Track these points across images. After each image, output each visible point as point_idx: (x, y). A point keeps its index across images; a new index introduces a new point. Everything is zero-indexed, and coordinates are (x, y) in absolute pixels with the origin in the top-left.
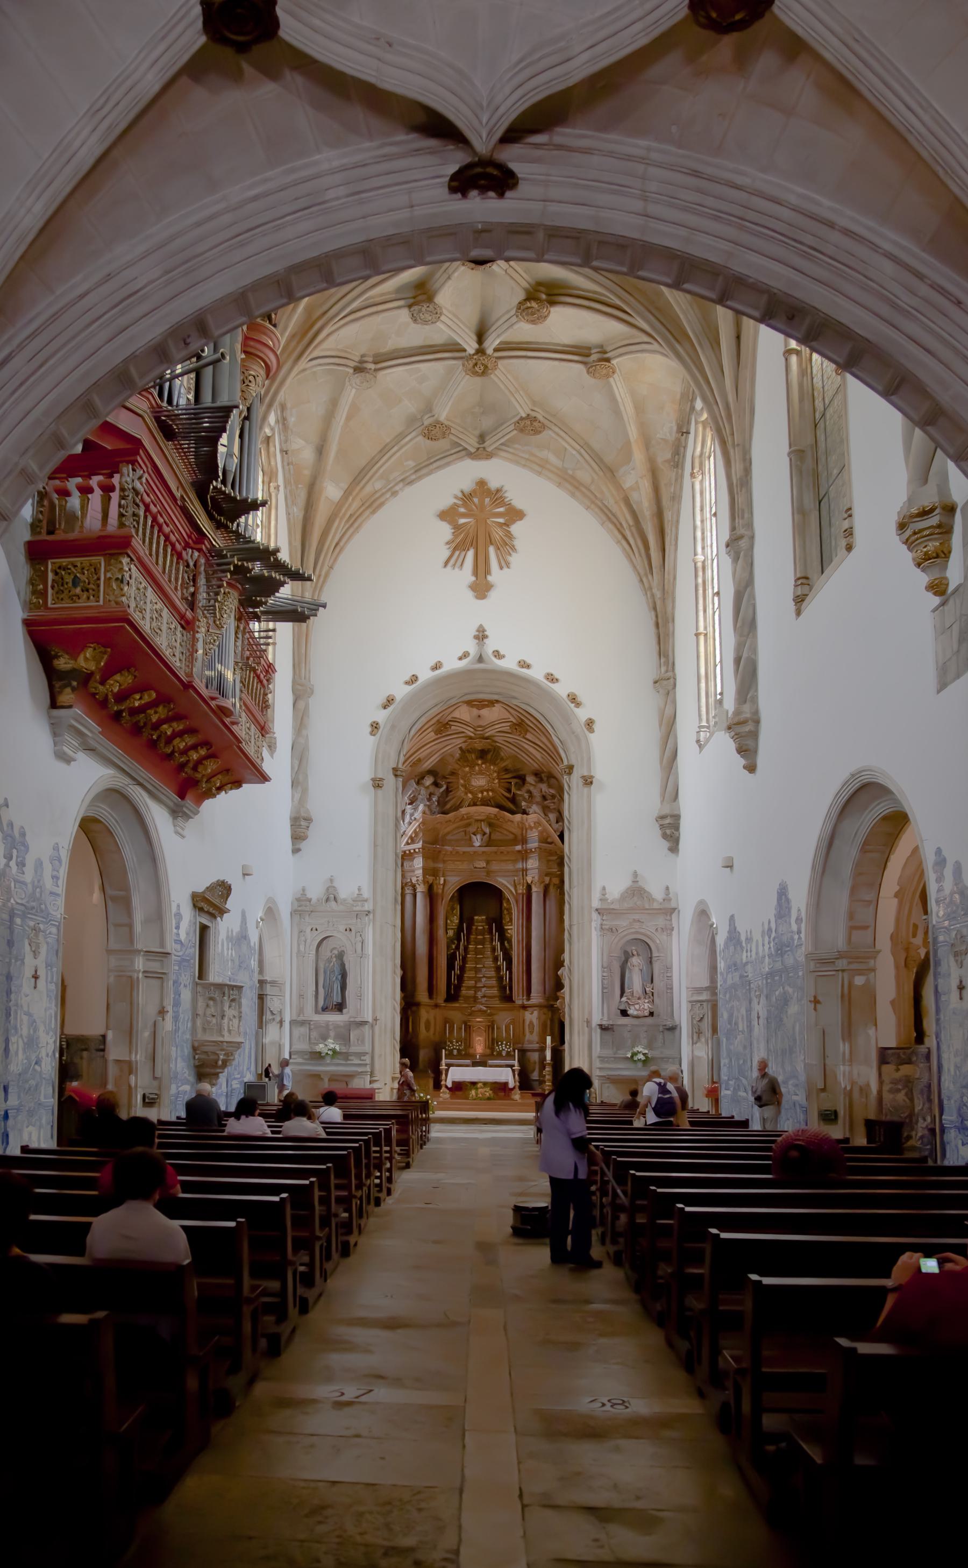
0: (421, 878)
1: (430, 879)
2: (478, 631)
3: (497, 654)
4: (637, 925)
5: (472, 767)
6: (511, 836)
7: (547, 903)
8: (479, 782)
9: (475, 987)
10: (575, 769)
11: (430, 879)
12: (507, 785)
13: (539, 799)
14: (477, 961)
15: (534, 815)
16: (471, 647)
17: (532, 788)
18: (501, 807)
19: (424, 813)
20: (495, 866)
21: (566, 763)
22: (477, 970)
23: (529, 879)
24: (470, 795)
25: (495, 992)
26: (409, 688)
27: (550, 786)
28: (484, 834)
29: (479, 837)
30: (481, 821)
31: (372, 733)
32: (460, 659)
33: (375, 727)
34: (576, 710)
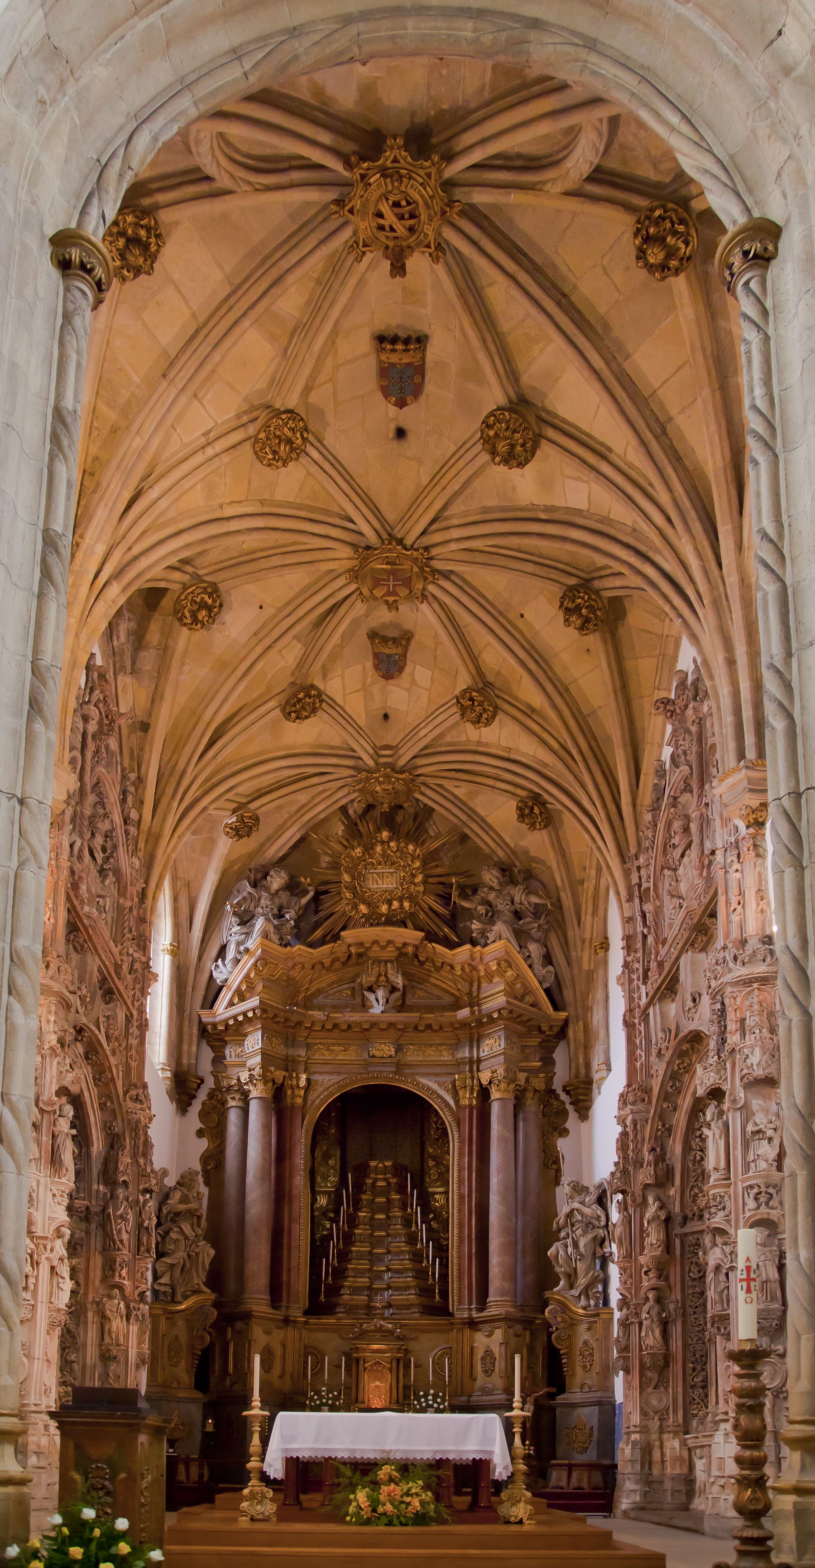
0: (258, 1071)
5: (368, 849)
6: (448, 999)
7: (521, 1125)
8: (383, 881)
9: (370, 1288)
12: (440, 889)
13: (508, 916)
14: (375, 1242)
15: (499, 944)
17: (492, 896)
18: (431, 937)
19: (265, 935)
20: (412, 1056)
22: (373, 1259)
24: (363, 908)
25: (411, 1297)
27: (529, 892)
28: (393, 989)
29: (381, 993)
30: (386, 962)
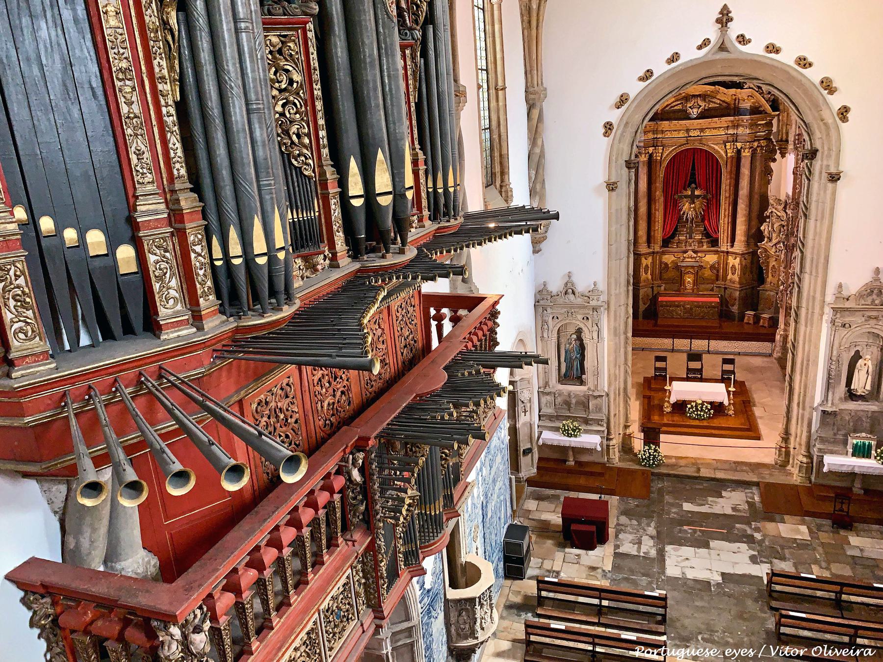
1: (651, 150)
2: (721, 13)
3: (743, 39)
4: (873, 322)
10: (819, 155)
11: (651, 150)
16: (713, 33)
20: (708, 133)
21: (808, 146)
23: (739, 145)
26: (643, 84)
29: (695, 110)
31: (606, 134)
32: (700, 48)
33: (608, 127)
34: (830, 98)
